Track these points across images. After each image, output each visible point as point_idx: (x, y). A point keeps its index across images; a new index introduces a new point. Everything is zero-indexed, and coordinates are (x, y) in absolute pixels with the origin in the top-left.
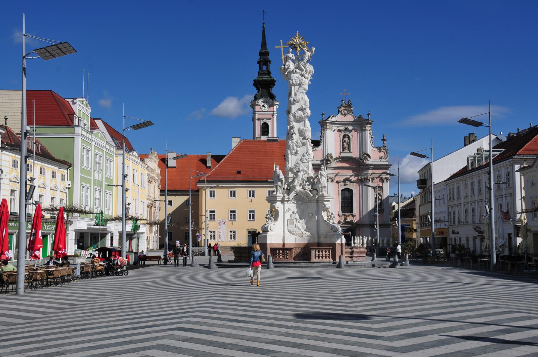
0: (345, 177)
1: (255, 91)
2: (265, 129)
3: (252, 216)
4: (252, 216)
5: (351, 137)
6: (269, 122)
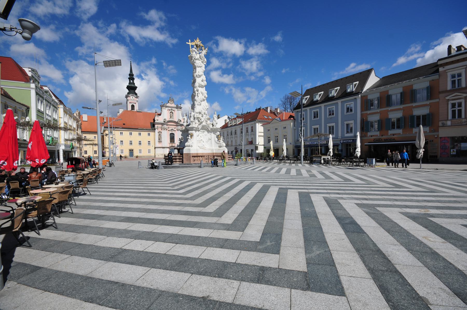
1: (128, 91)
2: (133, 107)
3: (131, 143)
4: (131, 143)
6: (134, 104)
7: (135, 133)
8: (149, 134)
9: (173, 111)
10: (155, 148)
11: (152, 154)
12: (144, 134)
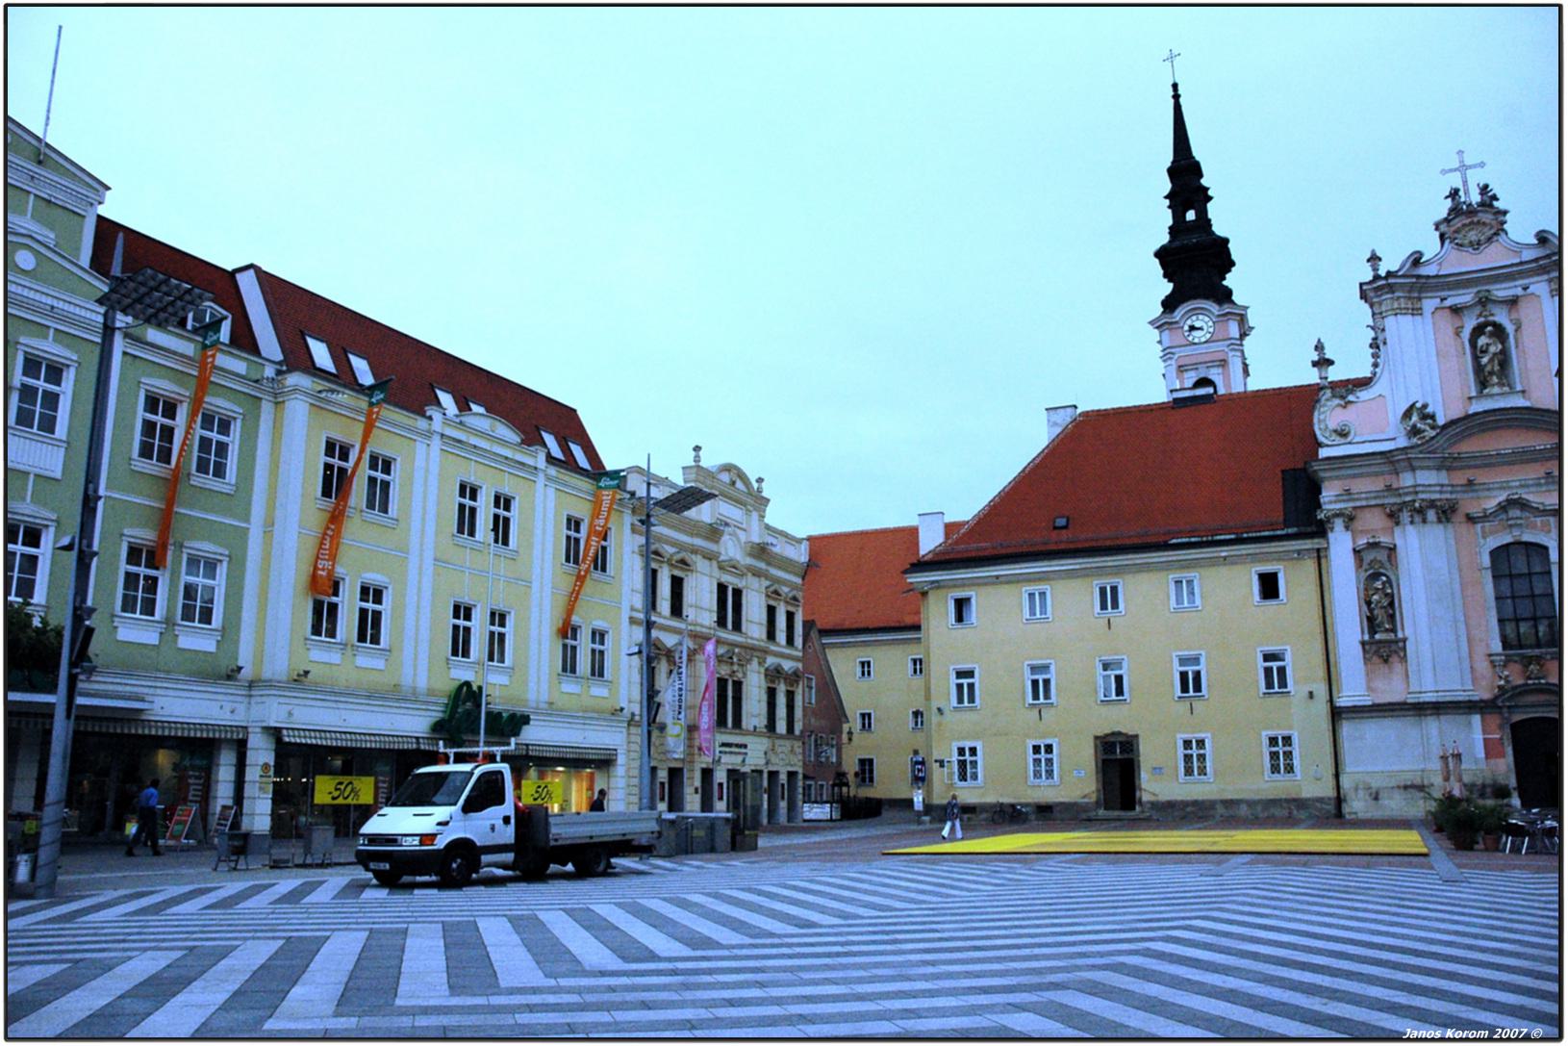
0: (1502, 497)
1: (1168, 288)
5: (1510, 328)
7: (1149, 590)
8: (1269, 587)
9: (1501, 316)
10: (1337, 714)
11: (1310, 781)
12: (1224, 585)
